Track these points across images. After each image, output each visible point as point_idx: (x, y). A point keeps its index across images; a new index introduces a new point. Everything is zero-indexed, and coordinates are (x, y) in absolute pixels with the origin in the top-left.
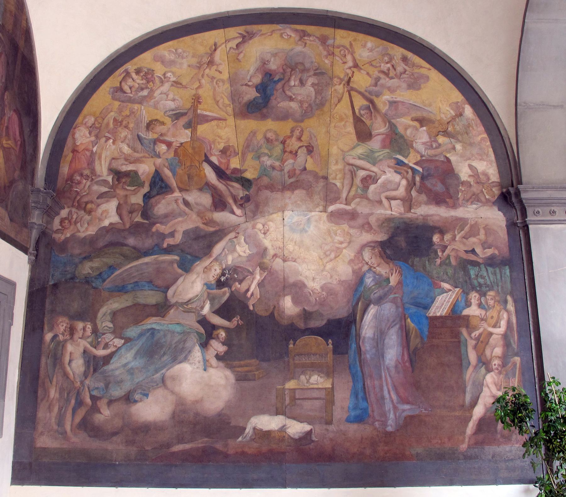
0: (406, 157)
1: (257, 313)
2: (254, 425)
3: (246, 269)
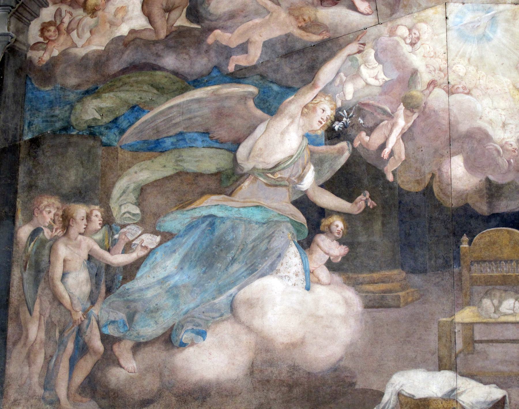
1: (402, 186)
2: (397, 387)
3: (378, 107)
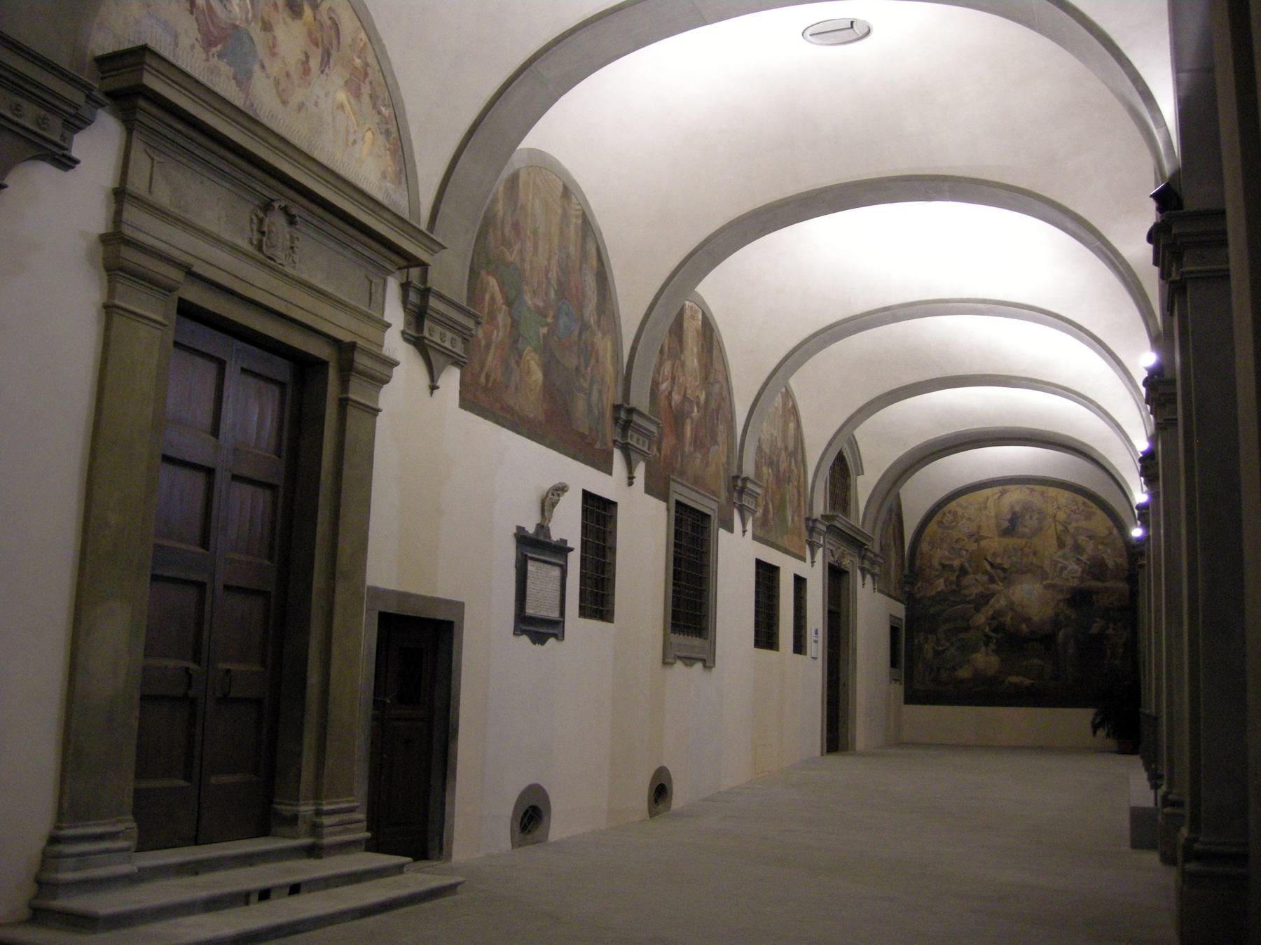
0: (1081, 556)
